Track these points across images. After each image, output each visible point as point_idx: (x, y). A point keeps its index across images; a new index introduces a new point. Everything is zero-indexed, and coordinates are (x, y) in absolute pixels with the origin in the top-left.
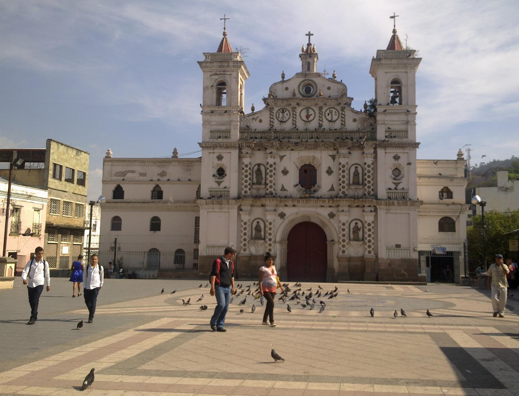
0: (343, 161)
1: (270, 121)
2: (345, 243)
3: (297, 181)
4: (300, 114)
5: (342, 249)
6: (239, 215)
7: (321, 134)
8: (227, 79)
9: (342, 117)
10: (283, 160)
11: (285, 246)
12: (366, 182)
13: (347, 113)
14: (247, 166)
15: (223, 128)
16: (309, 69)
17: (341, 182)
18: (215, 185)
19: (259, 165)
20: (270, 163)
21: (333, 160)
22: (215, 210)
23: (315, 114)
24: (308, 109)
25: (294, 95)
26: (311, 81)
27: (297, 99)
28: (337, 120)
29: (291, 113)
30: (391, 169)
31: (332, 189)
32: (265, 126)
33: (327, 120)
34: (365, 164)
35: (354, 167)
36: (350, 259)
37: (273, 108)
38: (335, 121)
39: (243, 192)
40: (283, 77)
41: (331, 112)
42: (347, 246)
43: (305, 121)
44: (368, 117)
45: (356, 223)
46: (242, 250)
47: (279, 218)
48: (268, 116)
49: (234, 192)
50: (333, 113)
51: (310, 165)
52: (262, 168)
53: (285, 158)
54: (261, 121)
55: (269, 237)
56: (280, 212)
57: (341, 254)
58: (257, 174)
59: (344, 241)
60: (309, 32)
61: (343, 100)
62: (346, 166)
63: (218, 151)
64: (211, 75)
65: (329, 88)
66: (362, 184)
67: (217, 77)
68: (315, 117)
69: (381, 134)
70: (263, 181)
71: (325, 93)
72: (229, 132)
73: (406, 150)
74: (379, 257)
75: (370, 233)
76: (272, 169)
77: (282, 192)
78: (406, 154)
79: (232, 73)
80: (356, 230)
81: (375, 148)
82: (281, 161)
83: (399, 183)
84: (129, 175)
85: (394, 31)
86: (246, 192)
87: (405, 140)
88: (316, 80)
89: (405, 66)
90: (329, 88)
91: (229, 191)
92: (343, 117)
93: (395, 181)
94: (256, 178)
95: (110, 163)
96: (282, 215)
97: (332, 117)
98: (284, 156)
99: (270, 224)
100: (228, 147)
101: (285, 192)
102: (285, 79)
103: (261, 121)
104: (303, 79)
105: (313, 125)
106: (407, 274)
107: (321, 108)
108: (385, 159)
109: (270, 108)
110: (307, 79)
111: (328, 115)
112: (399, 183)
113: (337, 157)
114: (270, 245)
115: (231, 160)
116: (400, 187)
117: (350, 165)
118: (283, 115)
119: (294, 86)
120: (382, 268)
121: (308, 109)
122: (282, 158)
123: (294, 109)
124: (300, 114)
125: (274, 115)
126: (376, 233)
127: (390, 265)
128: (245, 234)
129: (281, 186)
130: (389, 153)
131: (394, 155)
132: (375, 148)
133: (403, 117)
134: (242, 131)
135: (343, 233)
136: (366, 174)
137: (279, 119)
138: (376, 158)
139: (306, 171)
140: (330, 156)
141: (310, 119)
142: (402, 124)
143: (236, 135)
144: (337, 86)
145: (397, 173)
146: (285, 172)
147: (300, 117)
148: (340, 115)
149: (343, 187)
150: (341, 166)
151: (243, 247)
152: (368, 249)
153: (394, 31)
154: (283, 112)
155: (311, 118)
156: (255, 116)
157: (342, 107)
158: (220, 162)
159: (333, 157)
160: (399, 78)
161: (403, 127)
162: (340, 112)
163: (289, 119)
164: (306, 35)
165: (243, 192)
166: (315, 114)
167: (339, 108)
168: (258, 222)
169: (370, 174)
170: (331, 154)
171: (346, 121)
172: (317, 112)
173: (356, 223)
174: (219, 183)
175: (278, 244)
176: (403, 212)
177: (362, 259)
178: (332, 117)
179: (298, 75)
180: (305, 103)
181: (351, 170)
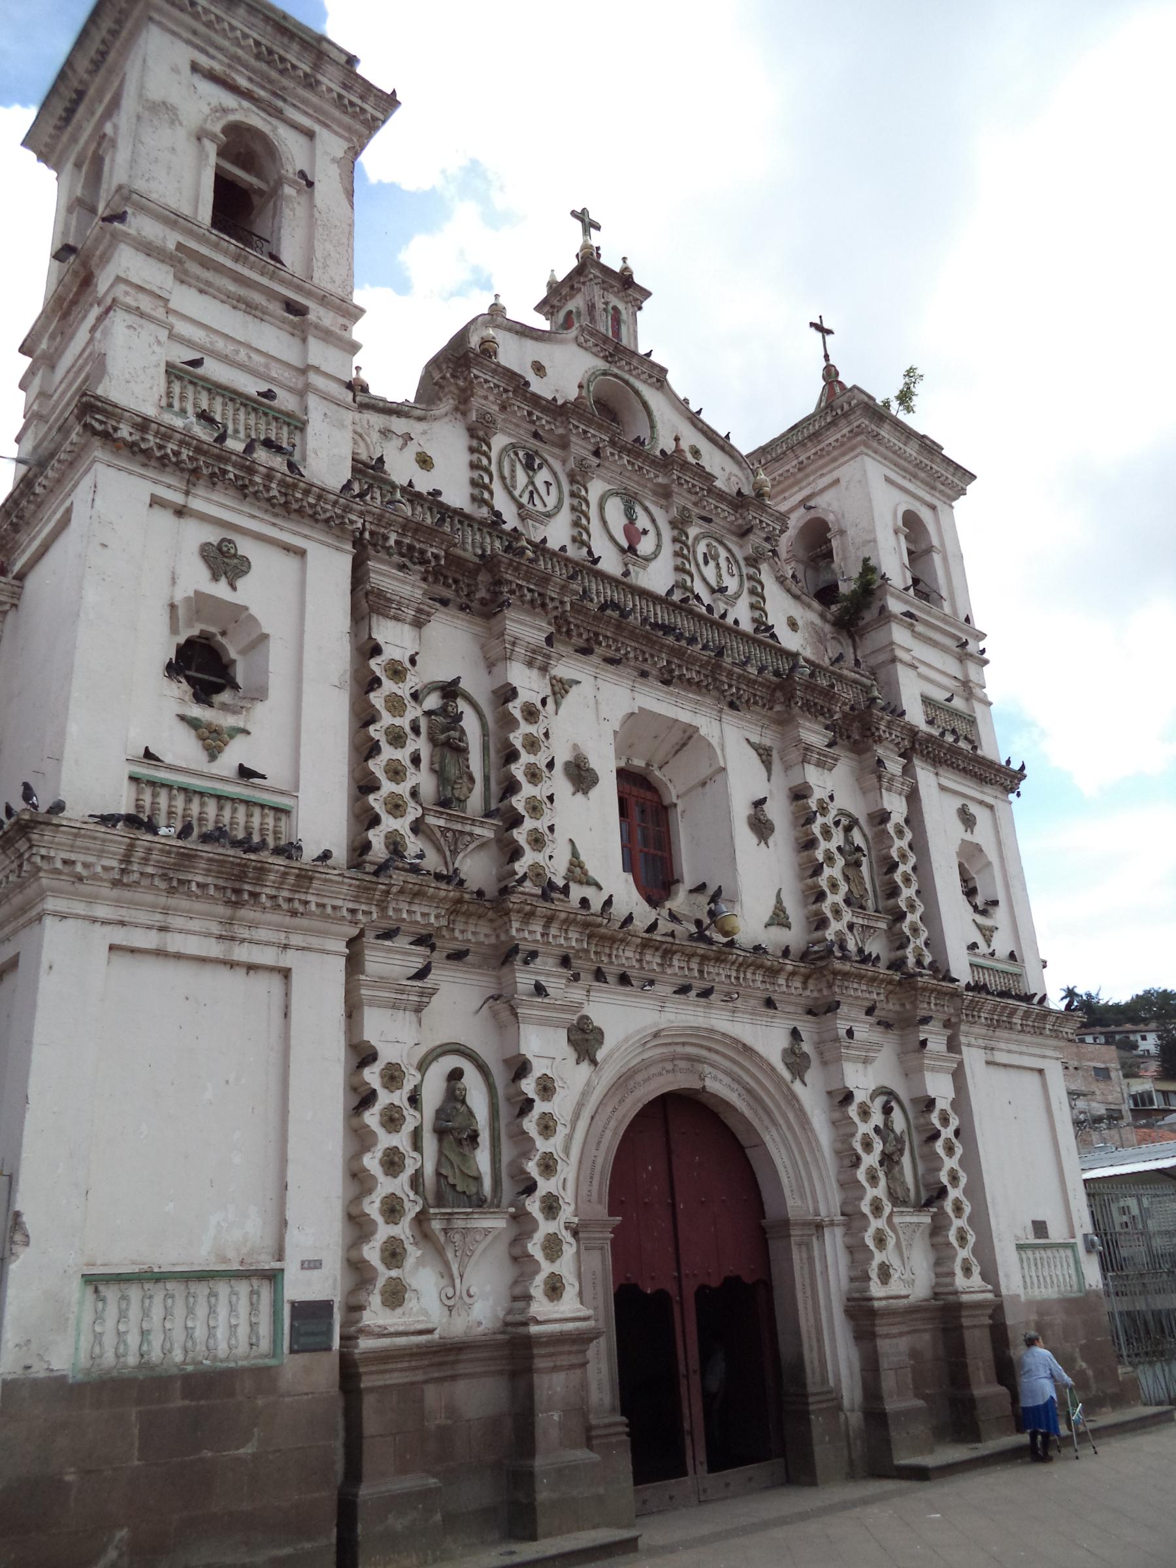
11: (599, 1263)
14: (397, 672)
18: (181, 750)
19: (450, 690)
22: (175, 943)
31: (779, 918)
41: (716, 558)
46: (375, 1300)
48: (464, 458)
53: (574, 690)
70: (475, 801)
74: (1004, 1292)
79: (317, 128)
91: (279, 810)
96: (585, 1039)
106: (1090, 1373)
115: (298, 600)
116: (1002, 944)
123: (578, 477)
133: (952, 666)
146: (581, 776)
148: (747, 585)
151: (384, 1274)
154: (529, 466)
155: (646, 546)
158: (220, 589)
159: (764, 754)
165: (376, 837)
168: (456, 1075)
172: (667, 534)
174: (213, 741)
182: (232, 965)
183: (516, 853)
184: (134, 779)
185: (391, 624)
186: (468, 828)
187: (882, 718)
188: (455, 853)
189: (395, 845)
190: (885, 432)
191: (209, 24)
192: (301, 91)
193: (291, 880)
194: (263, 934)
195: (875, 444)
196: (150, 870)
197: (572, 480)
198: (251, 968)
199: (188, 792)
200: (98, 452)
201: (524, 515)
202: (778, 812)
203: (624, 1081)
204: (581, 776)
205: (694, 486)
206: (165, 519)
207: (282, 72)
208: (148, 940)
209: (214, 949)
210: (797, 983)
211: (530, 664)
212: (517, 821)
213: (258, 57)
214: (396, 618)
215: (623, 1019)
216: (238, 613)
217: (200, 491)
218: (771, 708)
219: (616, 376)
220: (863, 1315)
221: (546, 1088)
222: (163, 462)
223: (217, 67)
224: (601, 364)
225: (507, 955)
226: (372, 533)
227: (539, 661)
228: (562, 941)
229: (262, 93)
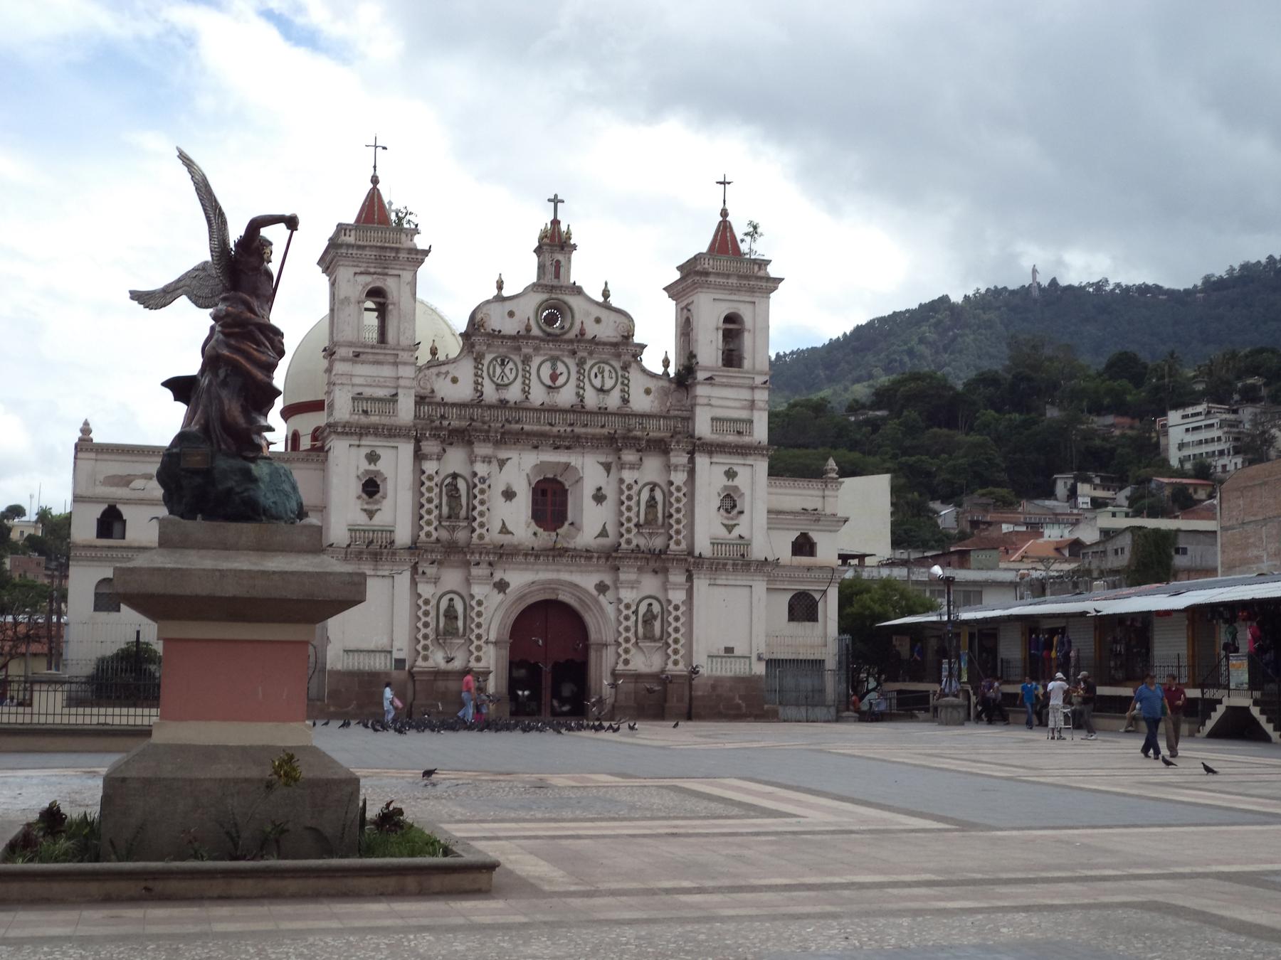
0: (628, 476)
1: (476, 383)
2: (629, 645)
5: (624, 656)
6: (414, 583)
9: (622, 383)
10: (504, 469)
11: (505, 653)
13: (634, 374)
14: (430, 478)
15: (381, 393)
16: (557, 275)
18: (362, 519)
19: (455, 476)
24: (554, 360)
25: (528, 329)
27: (535, 338)
31: (603, 533)
32: (463, 391)
33: (593, 386)
34: (671, 483)
36: (637, 677)
39: (422, 534)
40: (500, 286)
42: (633, 651)
43: (550, 387)
44: (673, 386)
45: (650, 605)
47: (496, 591)
49: (403, 536)
50: (606, 374)
51: (554, 481)
52: (461, 485)
54: (455, 380)
55: (477, 631)
56: (497, 577)
57: (620, 667)
58: (450, 497)
59: (627, 640)
60: (556, 196)
61: (625, 348)
63: (368, 441)
65: (598, 321)
67: (368, 279)
69: (703, 427)
70: (463, 513)
71: (592, 330)
73: (749, 461)
75: (678, 624)
78: (749, 469)
80: (649, 619)
81: (692, 454)
84: (138, 483)
85: (724, 213)
86: (428, 535)
88: (573, 301)
89: (752, 290)
90: (598, 321)
91: (391, 532)
93: (726, 522)
95: (93, 455)
96: (502, 586)
99: (480, 603)
100: (393, 433)
102: (505, 293)
103: (455, 380)
104: (545, 296)
105: (566, 397)
107: (581, 364)
109: (478, 354)
114: (479, 648)
115: (397, 463)
117: (640, 484)
119: (527, 310)
120: (700, 693)
121: (554, 360)
122: (502, 463)
123: (526, 360)
125: (485, 368)
126: (690, 624)
127: (714, 687)
128: (426, 625)
132: (692, 454)
134: (421, 400)
135: (625, 623)
138: (692, 472)
139: (544, 493)
142: (743, 408)
143: (406, 411)
144: (613, 316)
146: (509, 495)
147: (539, 377)
149: (629, 531)
150: (624, 487)
151: (423, 653)
152: (673, 657)
153: (724, 213)
154: (503, 364)
155: (561, 380)
156: (444, 369)
158: (372, 467)
159: (607, 467)
160: (741, 313)
161: (744, 414)
165: (422, 534)
167: (617, 365)
168: (451, 600)
169: (681, 505)
170: (603, 459)
171: (631, 392)
172: (574, 369)
173: (650, 605)
175: (491, 647)
176: (739, 583)
177: (662, 679)
183: (473, 530)
190: (711, 279)
197: (523, 362)
199: (364, 531)
200: (333, 436)
201: (499, 387)
202: (610, 492)
203: (522, 598)
204: (509, 495)
206: (354, 450)
210: (603, 560)
212: (475, 519)
215: (520, 579)
216: (378, 473)
220: (615, 675)
221: (480, 603)
224: (545, 296)
225: (467, 564)
227: (487, 460)
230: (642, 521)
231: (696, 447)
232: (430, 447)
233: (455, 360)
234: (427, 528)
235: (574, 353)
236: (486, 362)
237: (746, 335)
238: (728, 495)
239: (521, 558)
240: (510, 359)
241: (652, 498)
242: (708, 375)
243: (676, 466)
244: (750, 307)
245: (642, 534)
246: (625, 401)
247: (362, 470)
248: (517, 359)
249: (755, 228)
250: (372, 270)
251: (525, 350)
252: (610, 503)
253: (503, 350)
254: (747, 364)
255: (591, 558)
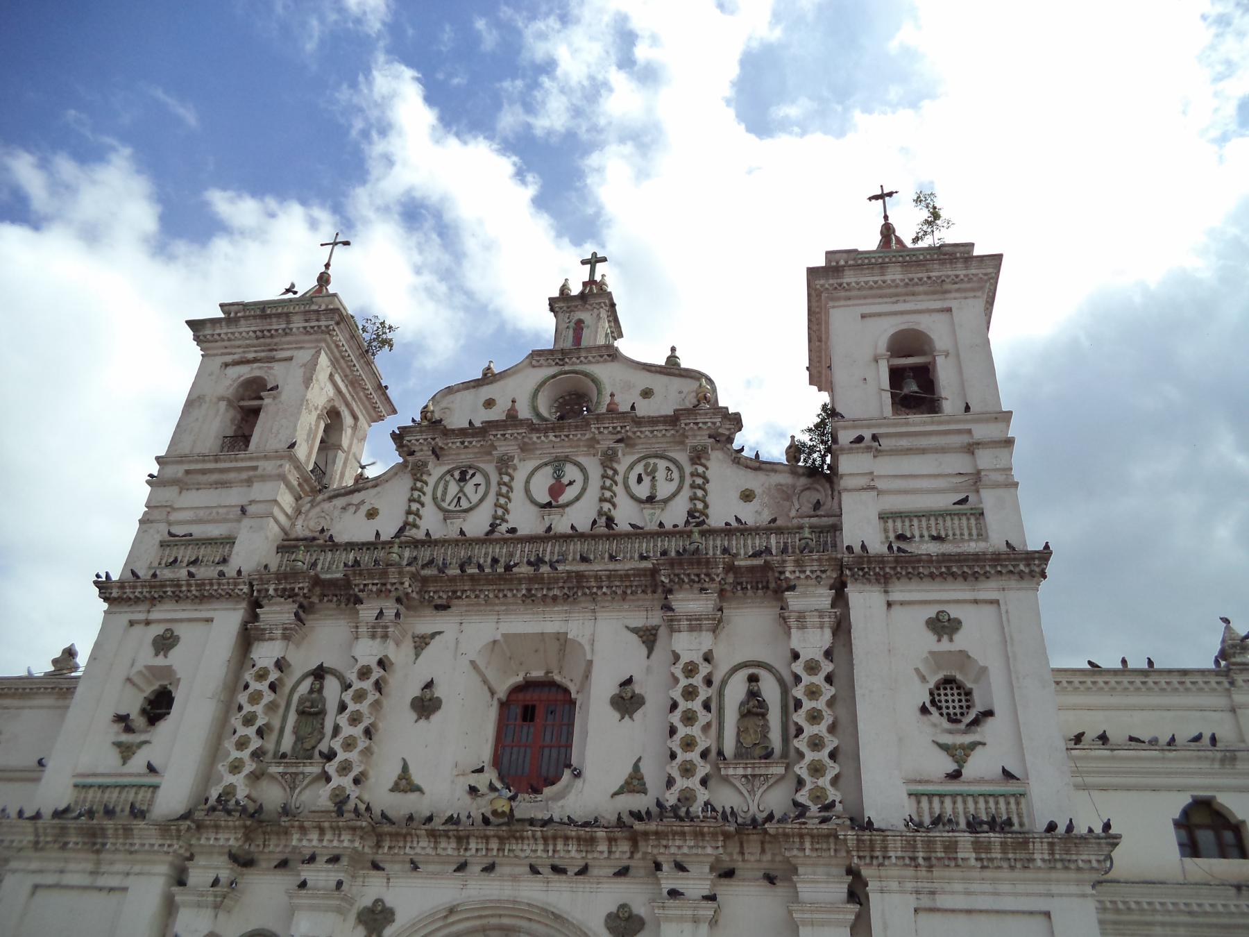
0: (688, 645)
3: (485, 753)
4: (527, 482)
7: (603, 546)
8: (275, 373)
10: (425, 653)
12: (801, 744)
13: (717, 466)
15: (215, 531)
16: (578, 338)
17: (675, 744)
20: (363, 661)
21: (644, 651)
22: (69, 879)
23: (586, 479)
24: (558, 464)
26: (586, 375)
27: (522, 423)
28: (674, 495)
29: (494, 478)
30: (923, 679)
31: (634, 783)
33: (633, 497)
35: (742, 675)
37: (425, 464)
38: (666, 501)
41: (652, 473)
49: (173, 796)
50: (661, 475)
53: (435, 643)
62: (704, 669)
63: (162, 612)
64: (226, 365)
65: (647, 394)
66: (785, 755)
68: (584, 489)
72: (229, 541)
73: (988, 590)
76: (368, 685)
77: (398, 796)
78: (989, 610)
79: (295, 353)
81: (839, 590)
82: (417, 655)
83: (973, 746)
87: (973, 547)
88: (602, 371)
92: (701, 484)
94: (296, 731)
97: (653, 487)
98: (433, 635)
101: (413, 796)
105: (580, 516)
107: (609, 459)
108: (891, 636)
110: (567, 368)
111: (640, 480)
112: (973, 746)
113: (663, 632)
116: (980, 766)
118: (461, 490)
121: (558, 464)
122: (422, 642)
123: (504, 465)
124: (527, 482)
129: (397, 770)
130: (902, 603)
131: (931, 612)
132: (839, 590)
133: (959, 463)
136: (798, 704)
137: (445, 505)
138: (842, 628)
139: (529, 714)
140: (635, 631)
141: (563, 499)
145: (954, 699)
146: (426, 705)
148: (688, 481)
150: (678, 671)
154: (463, 479)
157: (694, 449)
159: (649, 637)
162: (688, 469)
163: (481, 500)
164: (584, 262)
166: (586, 479)
169: (821, 704)
170: (639, 620)
176: (1009, 903)
178: (653, 487)
179: (537, 357)
180: (550, 444)
181: (728, 691)
182: (100, 889)
184: (76, 786)
185: (266, 644)
186: (301, 769)
187: (784, 561)
188: (293, 789)
189: (229, 791)
190: (849, 278)
191: (229, 340)
192: (284, 339)
193: (121, 832)
194: (119, 867)
195: (843, 294)
196: (49, 839)
198: (111, 889)
201: (447, 514)
205: (614, 428)
206: (138, 629)
207: (272, 336)
208: (50, 879)
209: (86, 880)
211: (373, 636)
213: (257, 338)
214: (271, 639)
217: (159, 607)
218: (654, 592)
219: (566, 373)
222: (137, 600)
223: (236, 357)
226: (259, 591)
227: (379, 631)
228: (335, 843)
229: (263, 354)
230: (729, 747)
231: (848, 569)
232: (277, 614)
233: (377, 482)
234: (230, 779)
235: (593, 442)
236: (432, 481)
237: (940, 361)
238: (948, 682)
239: (422, 847)
240: (478, 469)
241: (753, 694)
242: (854, 434)
243: (801, 617)
244: (943, 317)
245: (726, 779)
246: (696, 516)
247: (139, 666)
248: (490, 469)
249: (936, 215)
250: (251, 356)
251: (503, 448)
252: (650, 717)
253: (465, 458)
254: (950, 405)
255: (592, 841)
